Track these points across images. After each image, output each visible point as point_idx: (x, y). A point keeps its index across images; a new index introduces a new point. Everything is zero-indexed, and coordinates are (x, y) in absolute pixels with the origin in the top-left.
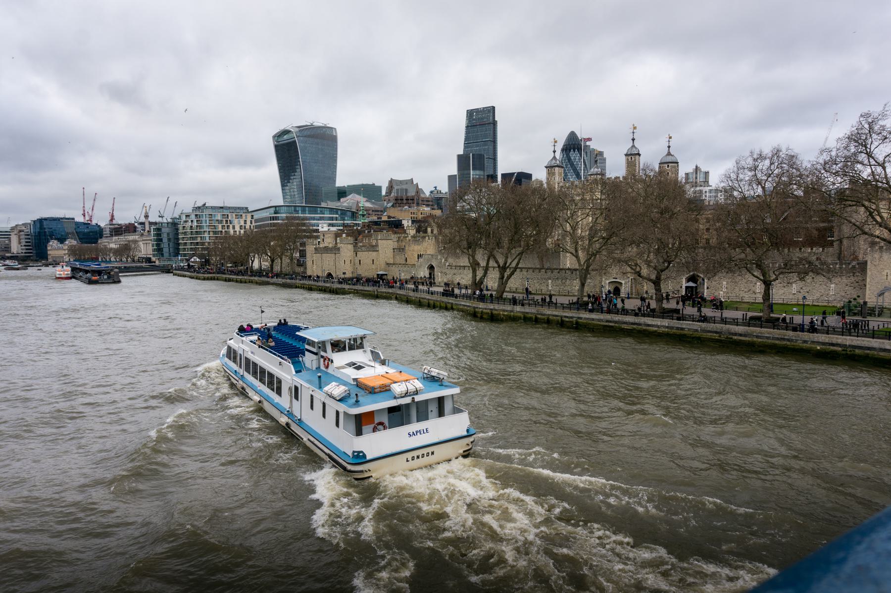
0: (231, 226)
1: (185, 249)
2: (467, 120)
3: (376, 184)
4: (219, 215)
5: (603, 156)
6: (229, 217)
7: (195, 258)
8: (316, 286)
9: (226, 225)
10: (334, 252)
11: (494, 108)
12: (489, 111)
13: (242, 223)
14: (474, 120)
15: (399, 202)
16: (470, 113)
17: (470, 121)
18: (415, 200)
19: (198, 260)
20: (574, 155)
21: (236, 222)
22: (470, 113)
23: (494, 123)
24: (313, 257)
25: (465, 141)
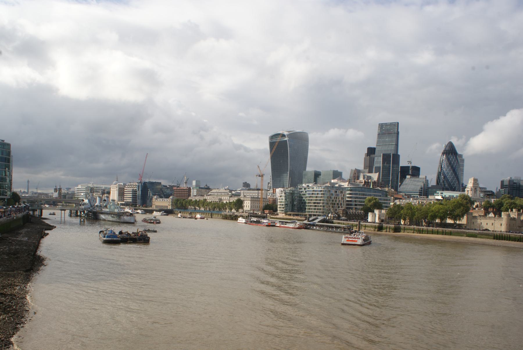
0: (338, 198)
1: (315, 208)
2: (378, 130)
3: (339, 171)
4: (333, 191)
5: (462, 158)
6: (337, 193)
7: (335, 214)
8: (515, 235)
9: (336, 197)
10: (494, 219)
11: (398, 123)
12: (395, 125)
13: (342, 196)
14: (383, 130)
15: (367, 184)
16: (381, 126)
17: (381, 131)
18: (377, 183)
19: (337, 216)
20: (451, 157)
21: (340, 195)
22: (381, 126)
23: (398, 133)
24: (471, 221)
25: (377, 144)
